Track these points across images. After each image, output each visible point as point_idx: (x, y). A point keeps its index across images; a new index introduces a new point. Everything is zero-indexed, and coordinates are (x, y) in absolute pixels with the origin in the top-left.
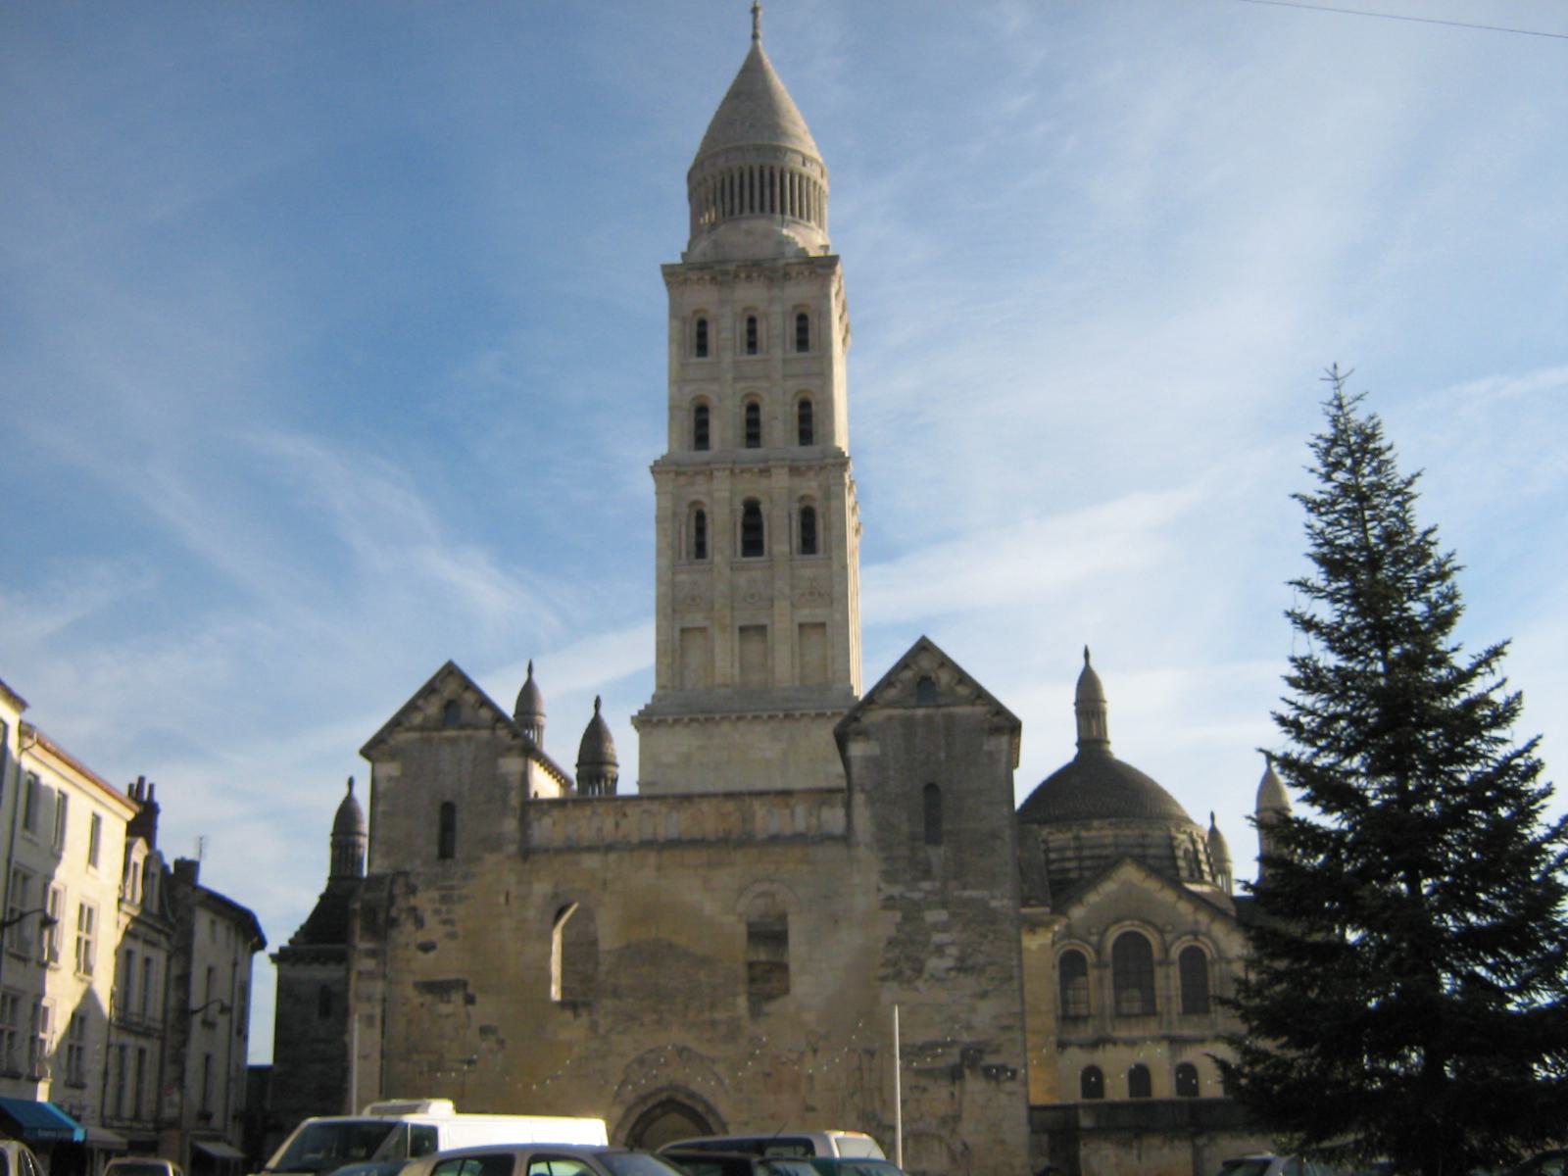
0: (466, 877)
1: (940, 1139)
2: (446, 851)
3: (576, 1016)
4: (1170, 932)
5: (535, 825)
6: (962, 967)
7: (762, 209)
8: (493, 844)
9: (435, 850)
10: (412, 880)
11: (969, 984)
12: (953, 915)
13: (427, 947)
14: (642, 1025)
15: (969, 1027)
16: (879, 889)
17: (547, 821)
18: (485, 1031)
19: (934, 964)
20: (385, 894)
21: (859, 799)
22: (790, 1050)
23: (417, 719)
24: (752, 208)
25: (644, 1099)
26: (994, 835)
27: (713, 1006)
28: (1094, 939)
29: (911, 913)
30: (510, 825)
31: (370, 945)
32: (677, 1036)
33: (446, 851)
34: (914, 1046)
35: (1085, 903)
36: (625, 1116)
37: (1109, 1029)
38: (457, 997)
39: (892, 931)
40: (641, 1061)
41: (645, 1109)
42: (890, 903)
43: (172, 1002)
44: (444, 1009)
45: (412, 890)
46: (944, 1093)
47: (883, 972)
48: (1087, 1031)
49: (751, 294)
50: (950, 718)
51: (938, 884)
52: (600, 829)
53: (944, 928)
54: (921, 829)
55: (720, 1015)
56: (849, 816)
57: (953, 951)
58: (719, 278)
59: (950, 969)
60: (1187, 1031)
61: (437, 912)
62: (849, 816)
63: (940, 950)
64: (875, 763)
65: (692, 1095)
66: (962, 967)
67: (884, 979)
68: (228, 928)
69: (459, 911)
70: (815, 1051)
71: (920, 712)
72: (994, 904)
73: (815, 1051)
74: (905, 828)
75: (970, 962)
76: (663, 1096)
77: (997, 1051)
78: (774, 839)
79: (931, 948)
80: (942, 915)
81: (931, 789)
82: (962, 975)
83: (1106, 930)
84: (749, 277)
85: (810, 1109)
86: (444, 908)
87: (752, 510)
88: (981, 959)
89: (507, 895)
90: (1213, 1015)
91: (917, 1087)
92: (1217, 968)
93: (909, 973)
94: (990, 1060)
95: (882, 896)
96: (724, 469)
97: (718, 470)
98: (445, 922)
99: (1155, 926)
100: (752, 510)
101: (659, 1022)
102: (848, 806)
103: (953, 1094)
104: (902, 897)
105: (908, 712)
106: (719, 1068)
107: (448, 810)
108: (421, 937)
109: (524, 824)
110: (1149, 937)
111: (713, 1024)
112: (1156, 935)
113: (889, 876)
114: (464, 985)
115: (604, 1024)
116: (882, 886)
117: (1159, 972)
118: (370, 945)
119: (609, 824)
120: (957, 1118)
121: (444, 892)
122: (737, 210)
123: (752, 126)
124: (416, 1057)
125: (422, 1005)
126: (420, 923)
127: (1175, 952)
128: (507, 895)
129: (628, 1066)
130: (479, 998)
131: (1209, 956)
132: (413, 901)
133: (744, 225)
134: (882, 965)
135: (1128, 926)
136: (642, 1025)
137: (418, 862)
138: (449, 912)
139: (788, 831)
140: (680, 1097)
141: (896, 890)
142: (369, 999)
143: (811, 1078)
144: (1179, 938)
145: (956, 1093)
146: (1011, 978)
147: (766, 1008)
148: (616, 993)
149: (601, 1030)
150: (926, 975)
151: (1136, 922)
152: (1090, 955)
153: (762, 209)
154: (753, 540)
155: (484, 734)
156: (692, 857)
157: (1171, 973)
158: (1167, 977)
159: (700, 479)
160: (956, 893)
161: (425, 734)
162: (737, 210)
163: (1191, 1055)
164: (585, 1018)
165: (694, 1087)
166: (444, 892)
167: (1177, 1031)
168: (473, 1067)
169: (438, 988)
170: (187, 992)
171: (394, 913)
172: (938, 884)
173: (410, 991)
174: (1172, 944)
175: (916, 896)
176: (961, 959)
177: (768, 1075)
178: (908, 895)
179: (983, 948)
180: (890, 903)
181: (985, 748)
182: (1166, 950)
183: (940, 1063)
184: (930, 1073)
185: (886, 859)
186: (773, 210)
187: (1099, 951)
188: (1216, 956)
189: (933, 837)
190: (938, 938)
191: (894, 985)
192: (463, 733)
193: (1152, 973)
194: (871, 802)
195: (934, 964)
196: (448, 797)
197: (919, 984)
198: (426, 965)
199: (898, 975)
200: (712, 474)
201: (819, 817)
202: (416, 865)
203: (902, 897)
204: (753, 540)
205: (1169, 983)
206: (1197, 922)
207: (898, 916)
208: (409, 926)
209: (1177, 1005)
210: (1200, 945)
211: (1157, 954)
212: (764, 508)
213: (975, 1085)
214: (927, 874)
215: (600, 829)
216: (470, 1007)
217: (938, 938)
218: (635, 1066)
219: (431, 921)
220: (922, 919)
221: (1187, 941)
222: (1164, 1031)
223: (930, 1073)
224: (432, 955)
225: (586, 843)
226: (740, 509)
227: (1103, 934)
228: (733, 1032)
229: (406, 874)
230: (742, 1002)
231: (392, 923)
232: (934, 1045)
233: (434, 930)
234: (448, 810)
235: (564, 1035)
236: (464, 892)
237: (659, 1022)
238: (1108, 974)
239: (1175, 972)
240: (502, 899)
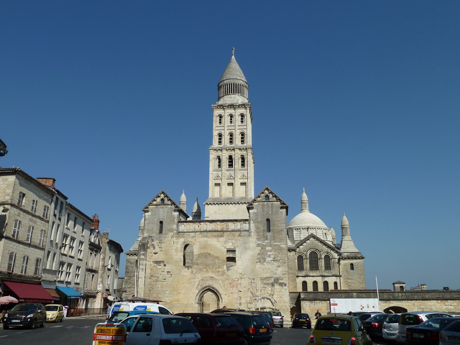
0: (165, 238)
1: (269, 299)
2: (161, 231)
3: (188, 269)
5: (180, 226)
6: (274, 260)
7: (234, 93)
8: (171, 230)
9: (158, 231)
10: (153, 238)
11: (276, 264)
12: (272, 248)
13: (155, 253)
14: (203, 272)
15: (276, 274)
16: (256, 242)
17: (183, 226)
18: (168, 272)
19: (268, 259)
20: (147, 241)
21: (252, 222)
22: (236, 278)
23: (155, 203)
24: (232, 93)
25: (203, 288)
26: (282, 231)
27: (219, 268)
29: (263, 247)
30: (175, 226)
31: (143, 253)
32: (211, 274)
33: (161, 231)
34: (263, 278)
36: (199, 292)
37: (308, 273)
38: (162, 264)
39: (259, 252)
40: (203, 280)
41: (203, 291)
42: (258, 245)
43: (101, 264)
44: (159, 267)
45: (153, 240)
46: (270, 289)
47: (257, 261)
48: (303, 273)
49: (231, 111)
50: (273, 203)
51: (269, 241)
52: (194, 228)
53: (271, 251)
54: (266, 228)
55: (220, 270)
56: (249, 225)
57: (272, 256)
58: (224, 107)
59: (272, 260)
60: (326, 274)
61: (158, 245)
62: (249, 225)
63: (269, 256)
64: (255, 213)
65: (213, 288)
66: (274, 260)
67: (257, 262)
68: (114, 248)
69: (163, 245)
70: (241, 278)
71: (266, 203)
72: (281, 246)
73: (241, 278)
74: (262, 228)
75: (276, 259)
76: (207, 288)
77: (282, 279)
78: (233, 231)
79: (268, 256)
80: (270, 248)
81: (268, 220)
82: (274, 262)
83: (308, 251)
84: (231, 107)
85: (241, 292)
86: (160, 244)
87: (230, 157)
88: (279, 258)
89: (174, 242)
90: (332, 270)
91: (264, 287)
92: (332, 260)
93: (263, 261)
94: (280, 281)
95: (257, 244)
96: (225, 149)
97: (223, 149)
98: (160, 248)
101: (206, 271)
102: (249, 223)
103: (272, 289)
104: (261, 244)
105: (263, 203)
106: (220, 282)
107: (161, 222)
108: (154, 251)
109: (178, 226)
111: (219, 271)
113: (258, 239)
114: (164, 262)
115: (194, 271)
116: (257, 241)
117: (320, 261)
118: (143, 253)
119: (197, 227)
120: (273, 295)
121: (160, 241)
122: (228, 93)
123: (232, 74)
124: (152, 278)
125: (154, 266)
126: (154, 248)
127: (323, 257)
128: (174, 242)
129: (200, 281)
130: (167, 265)
131: (331, 258)
132: (153, 243)
133: (230, 96)
134: (257, 259)
136: (203, 272)
137: (154, 234)
138: (161, 245)
139: (236, 229)
140: (211, 288)
141: (260, 242)
142: (142, 265)
143: (240, 284)
145: (273, 289)
146: (285, 263)
147: (230, 268)
148: (197, 264)
149: (194, 273)
150: (266, 262)
151: (314, 249)
152: (304, 257)
153: (234, 93)
154: (231, 165)
155: (170, 206)
156: (215, 234)
157: (322, 261)
158: (321, 262)
159: (219, 151)
160: (273, 243)
161: (156, 206)
162: (228, 93)
163: (326, 279)
164: (190, 270)
165: (214, 286)
166: (160, 241)
167: (323, 274)
168: (165, 281)
169: (158, 262)
170: (104, 262)
171: (148, 245)
172: (269, 241)
173: (152, 263)
174: (322, 255)
175: (264, 244)
176: (274, 258)
177: (231, 283)
178: (262, 243)
179: (279, 256)
180: (258, 245)
181: (280, 211)
182: (321, 256)
183: (269, 282)
184: (267, 284)
185: (257, 235)
186: (236, 93)
187: (306, 256)
189: (269, 230)
190: (269, 253)
191: (259, 263)
192: (165, 206)
194: (254, 222)
195: (268, 259)
196: (161, 220)
197: (265, 263)
198: (156, 258)
199: (260, 261)
200: (222, 150)
201: (243, 226)
202: (154, 235)
203: (261, 244)
204: (231, 165)
205: (322, 263)
207: (260, 248)
208: (152, 248)
209: (323, 268)
212: (233, 157)
213: (277, 287)
214: (267, 239)
215: (194, 228)
216: (165, 267)
217: (269, 253)
218: (201, 281)
219: (157, 247)
220: (266, 249)
221: (325, 254)
222: (320, 274)
223: (267, 284)
224: (157, 255)
225: (191, 231)
228: (223, 274)
229: (151, 237)
230: (225, 267)
231: (148, 248)
232: (269, 277)
233: (157, 249)
234: (161, 222)
235: (185, 274)
236: (164, 241)
237: (206, 271)
238: (308, 260)
239: (323, 260)
240: (173, 243)
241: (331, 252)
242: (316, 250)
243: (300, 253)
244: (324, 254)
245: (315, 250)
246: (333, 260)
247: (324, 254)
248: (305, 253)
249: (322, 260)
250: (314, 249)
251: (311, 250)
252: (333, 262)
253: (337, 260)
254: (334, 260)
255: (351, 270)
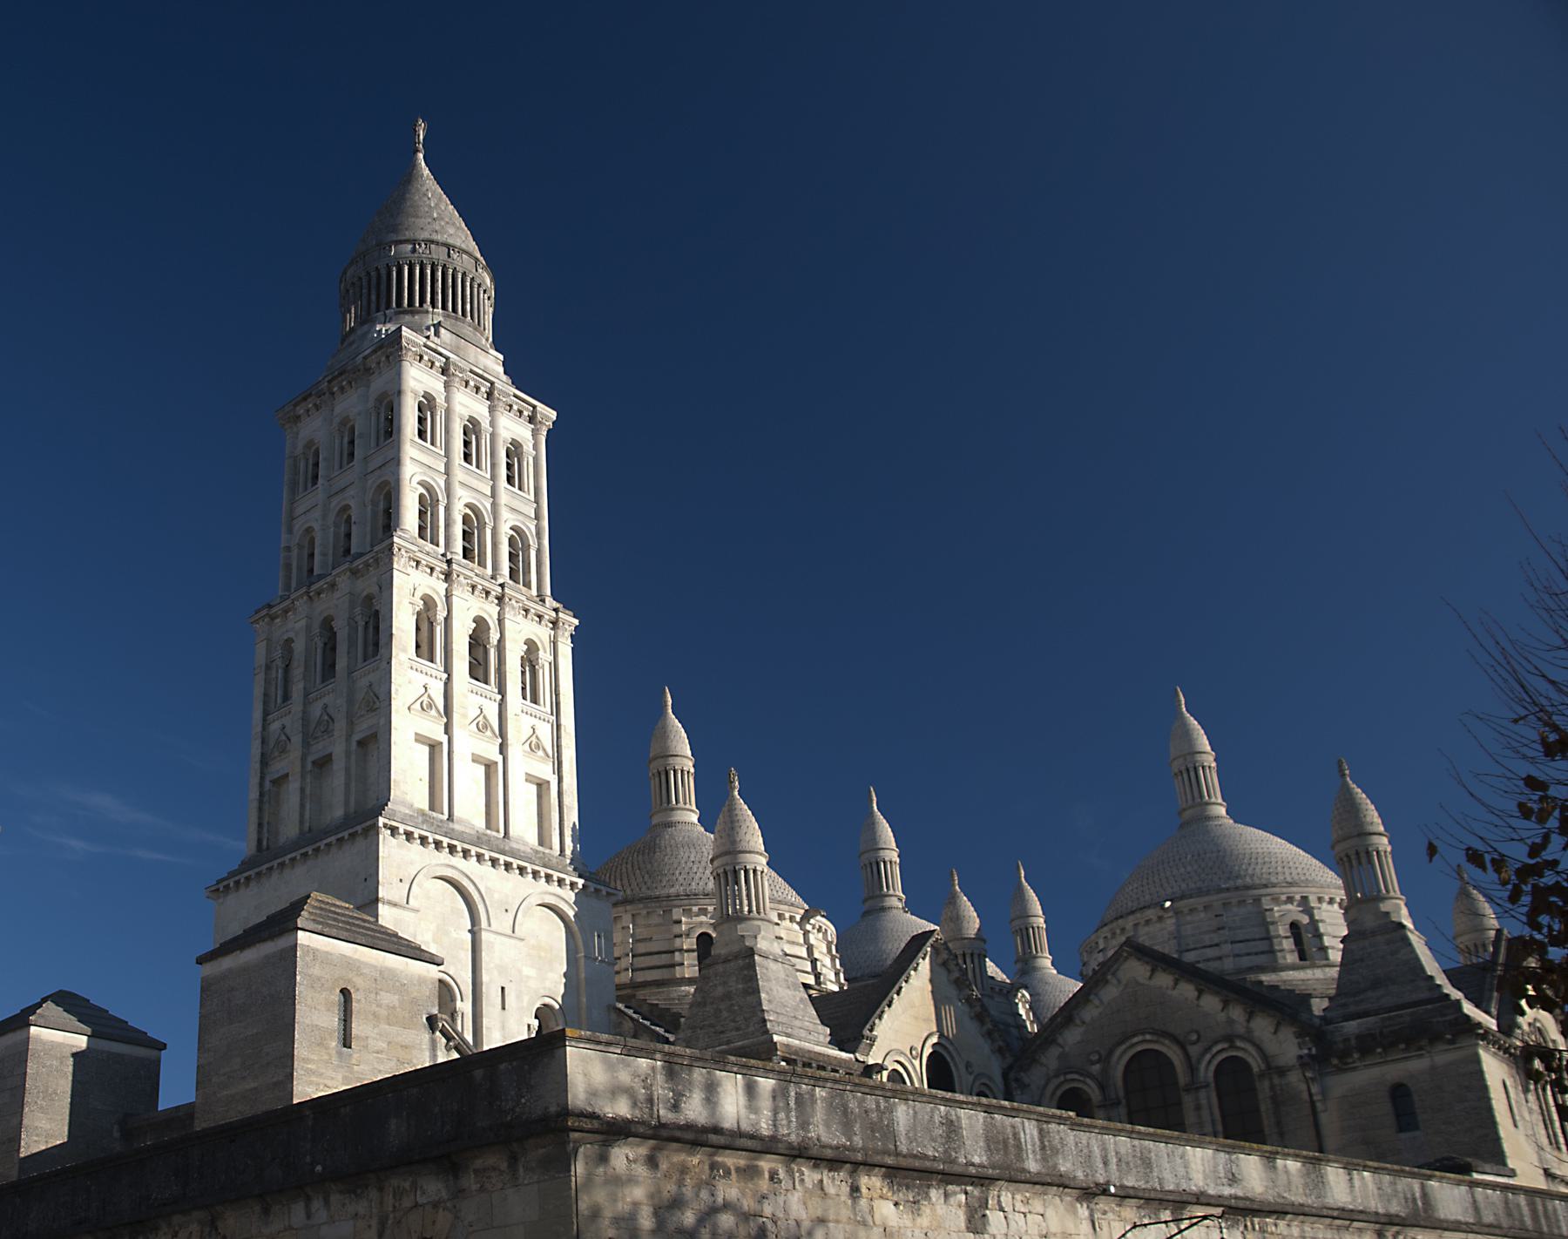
4: (1194, 1043)
28: (1096, 1068)
35: (1078, 1022)
83: (1111, 1052)
92: (1266, 1084)
96: (301, 596)
99: (1175, 1039)
100: (327, 625)
110: (1170, 1054)
112: (1176, 1048)
117: (1188, 1100)
127: (1206, 1072)
131: (1256, 1070)
135: (1140, 1043)
144: (1208, 1049)
151: (1148, 1037)
158: (1198, 1108)
174: (1199, 1061)
182: (1192, 1069)
187: (1102, 1087)
188: (1263, 1067)
193: (1179, 1103)
206: (1231, 1022)
210: (1240, 1054)
211: (1183, 1078)
221: (1221, 1052)
226: (316, 630)
227: (1105, 1059)
241: (1249, 1031)
242: (1162, 1039)
243: (1069, 1076)
244: (1208, 1057)
245: (1155, 1038)
246: (1272, 1088)
247: (1208, 1057)
248: (1096, 1068)
249: (1202, 1094)
250: (1148, 1037)
251: (1128, 1044)
252: (1274, 1099)
253: (1294, 1078)
254: (1276, 1081)
255: (1401, 1130)
